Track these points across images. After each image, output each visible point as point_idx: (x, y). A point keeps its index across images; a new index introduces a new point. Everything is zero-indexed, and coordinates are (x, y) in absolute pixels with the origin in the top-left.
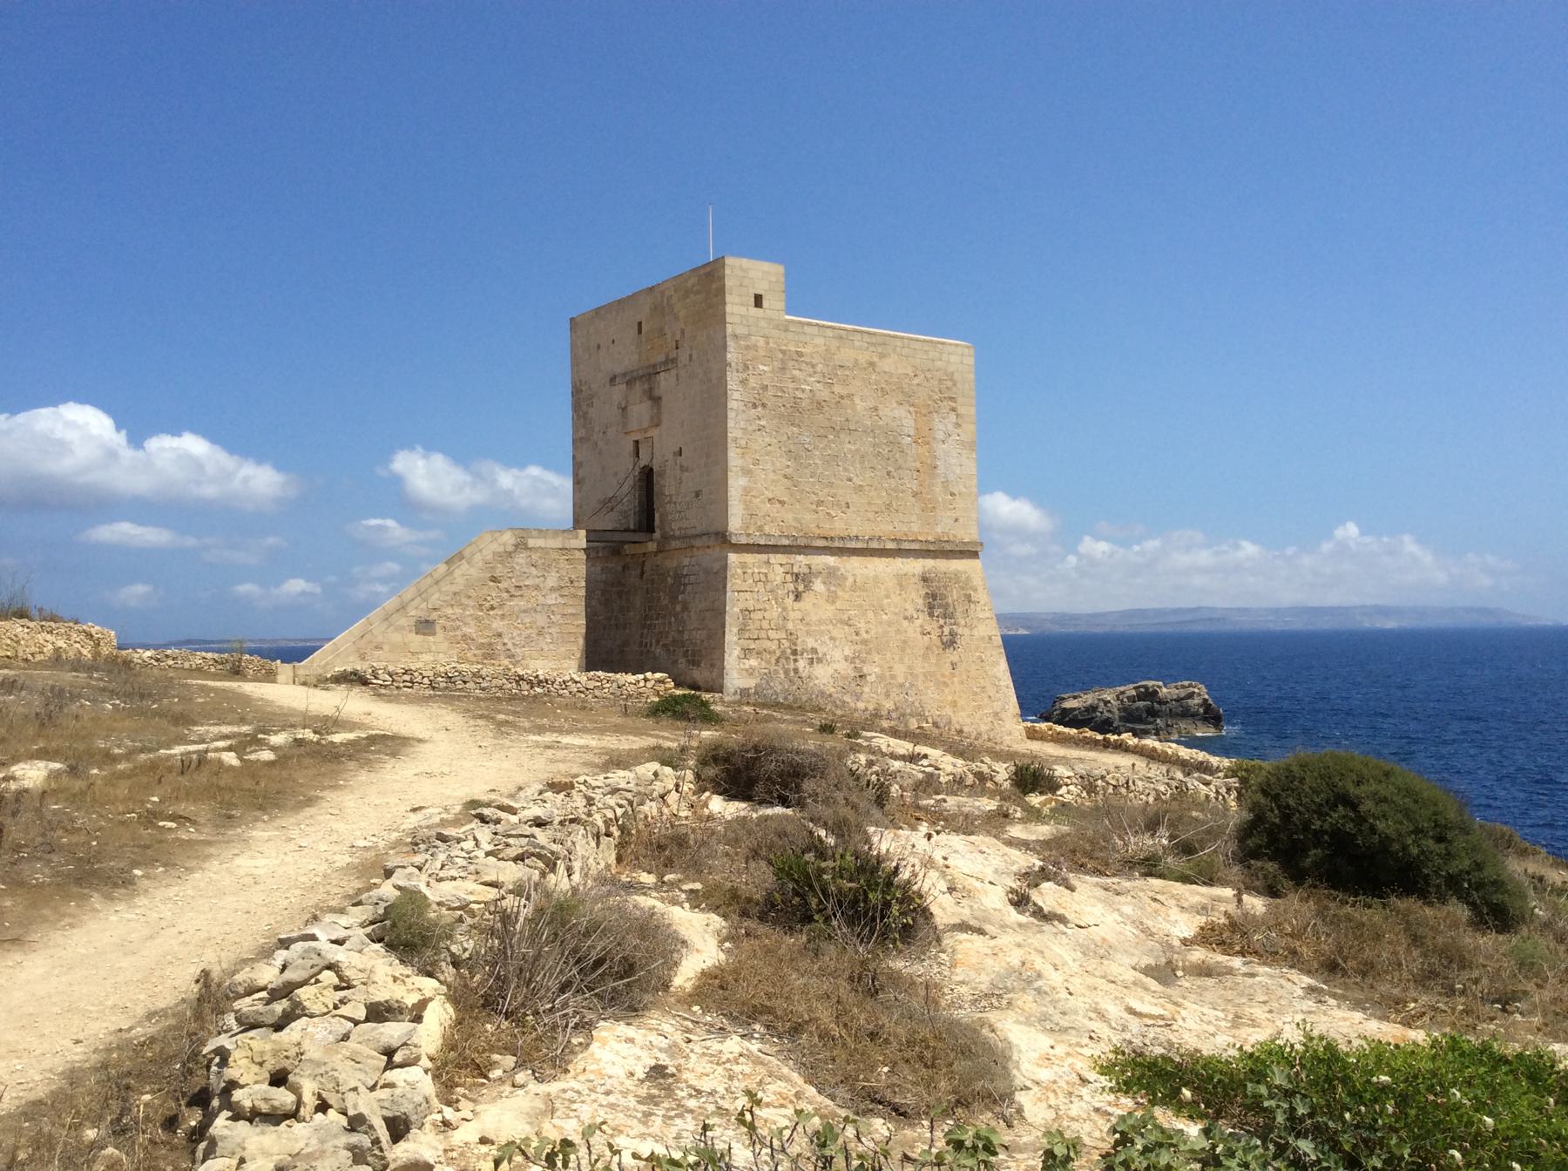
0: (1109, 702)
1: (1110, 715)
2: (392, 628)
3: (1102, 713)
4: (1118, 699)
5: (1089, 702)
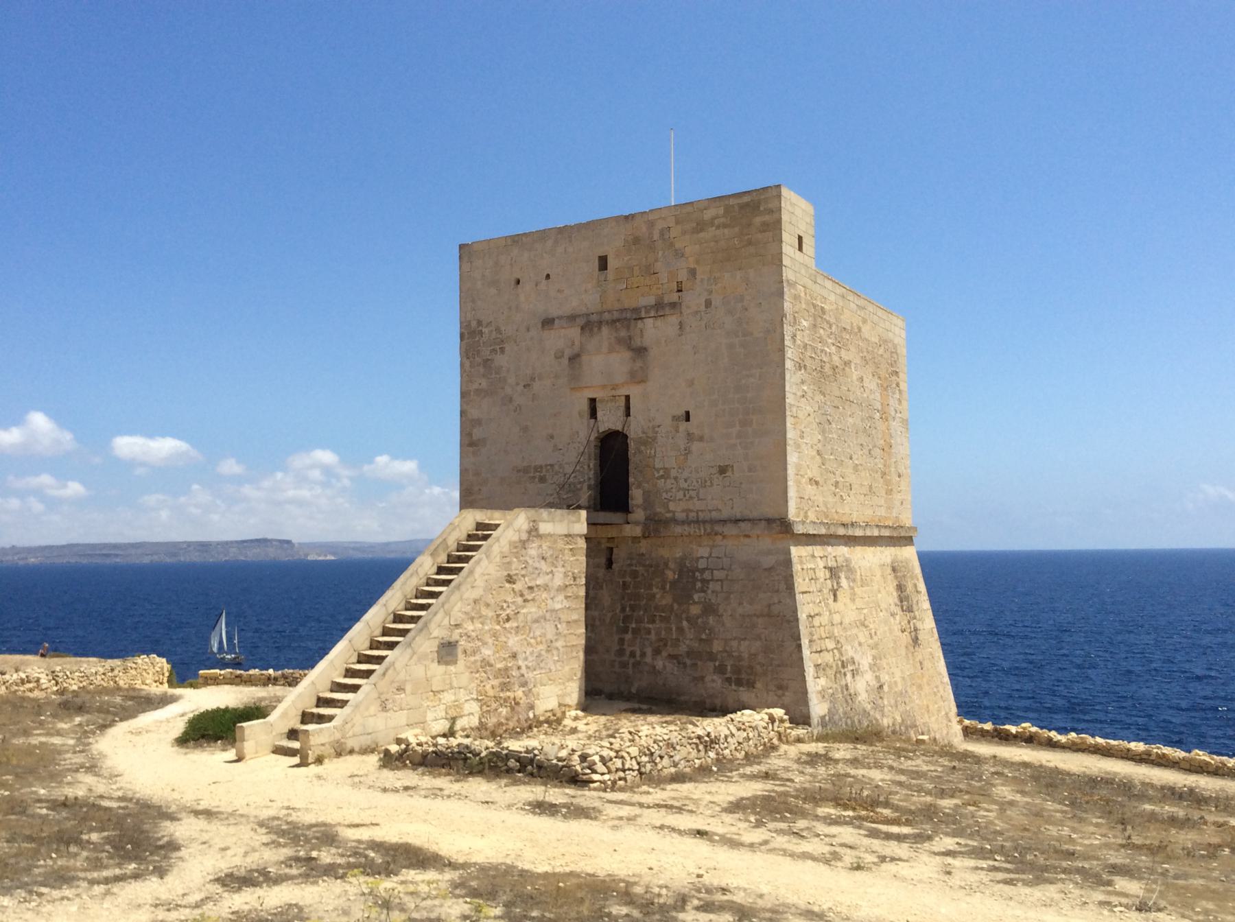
2: (415, 657)
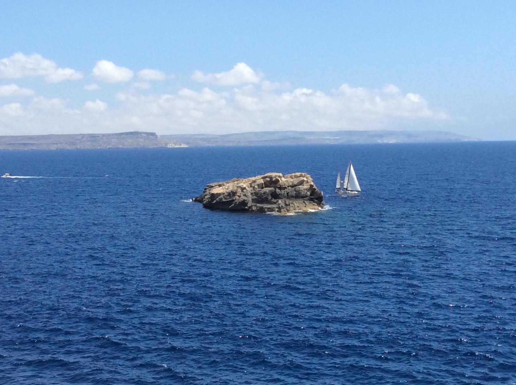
0: (245, 188)
1: (245, 198)
3: (239, 196)
4: (251, 186)
5: (231, 189)
